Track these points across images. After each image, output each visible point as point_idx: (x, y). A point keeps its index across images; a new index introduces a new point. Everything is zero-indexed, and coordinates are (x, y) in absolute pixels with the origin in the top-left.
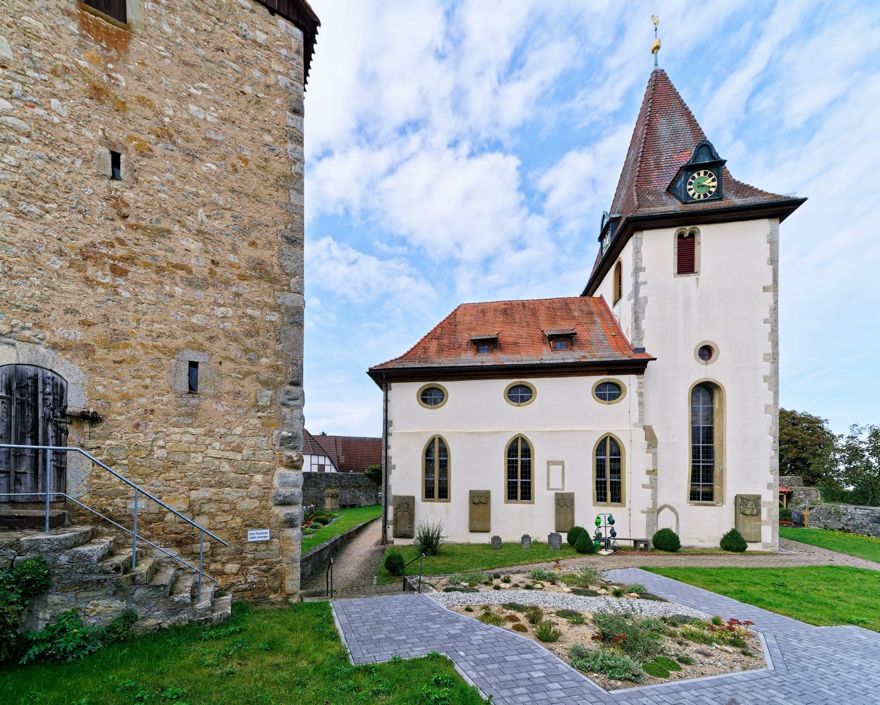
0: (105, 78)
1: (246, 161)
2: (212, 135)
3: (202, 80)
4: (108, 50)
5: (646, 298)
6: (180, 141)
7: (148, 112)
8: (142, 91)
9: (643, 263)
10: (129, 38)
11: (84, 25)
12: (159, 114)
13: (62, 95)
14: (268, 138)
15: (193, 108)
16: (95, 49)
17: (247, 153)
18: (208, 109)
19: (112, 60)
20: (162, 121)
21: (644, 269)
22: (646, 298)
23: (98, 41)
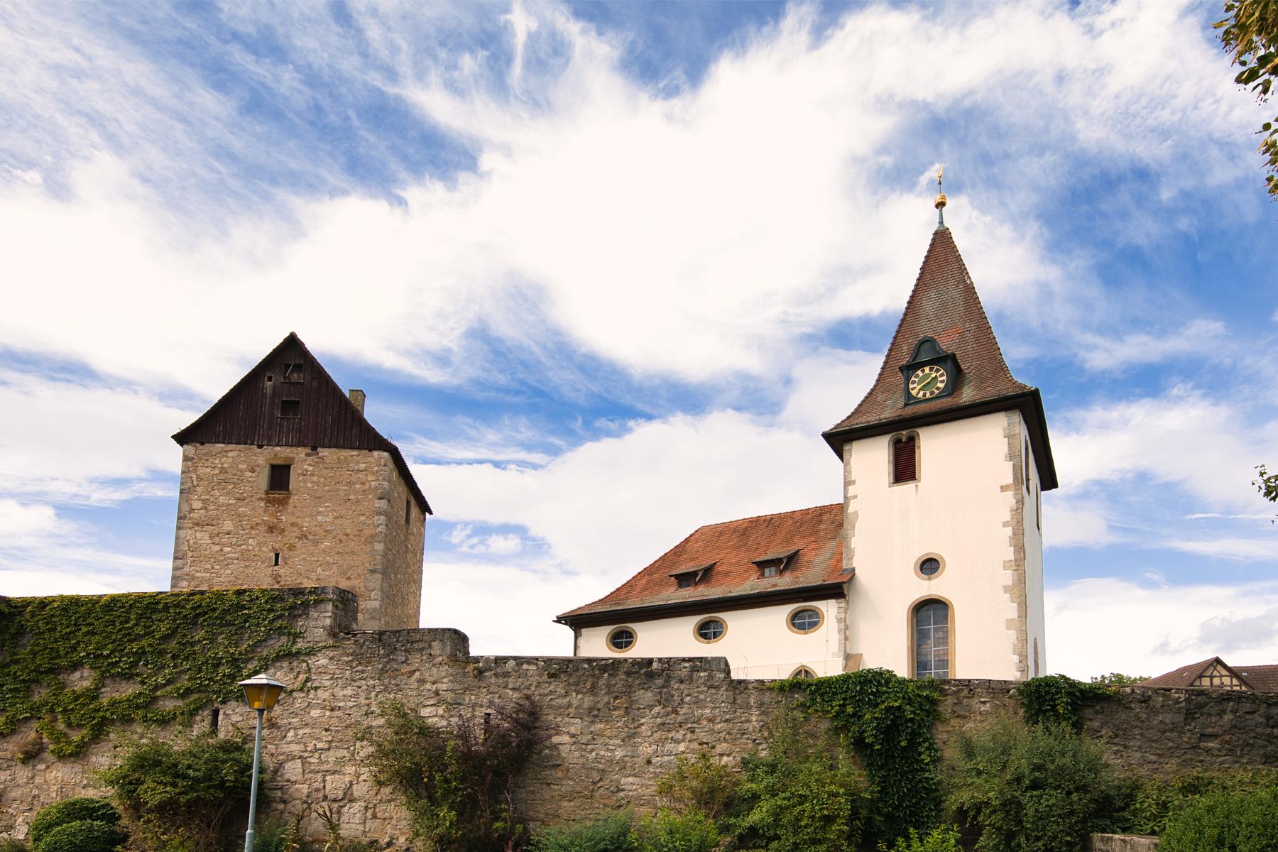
0: (276, 520)
1: (347, 535)
2: (329, 528)
3: (326, 502)
4: (278, 508)
5: (856, 513)
6: (311, 537)
7: (295, 529)
8: (294, 520)
9: (853, 476)
10: (289, 498)
11: (268, 501)
12: (301, 528)
13: (254, 536)
14: (362, 518)
15: (320, 518)
16: (272, 509)
17: (349, 531)
18: (328, 515)
19: (280, 511)
20: (302, 531)
21: (854, 482)
22: (856, 513)
23: (273, 506)
